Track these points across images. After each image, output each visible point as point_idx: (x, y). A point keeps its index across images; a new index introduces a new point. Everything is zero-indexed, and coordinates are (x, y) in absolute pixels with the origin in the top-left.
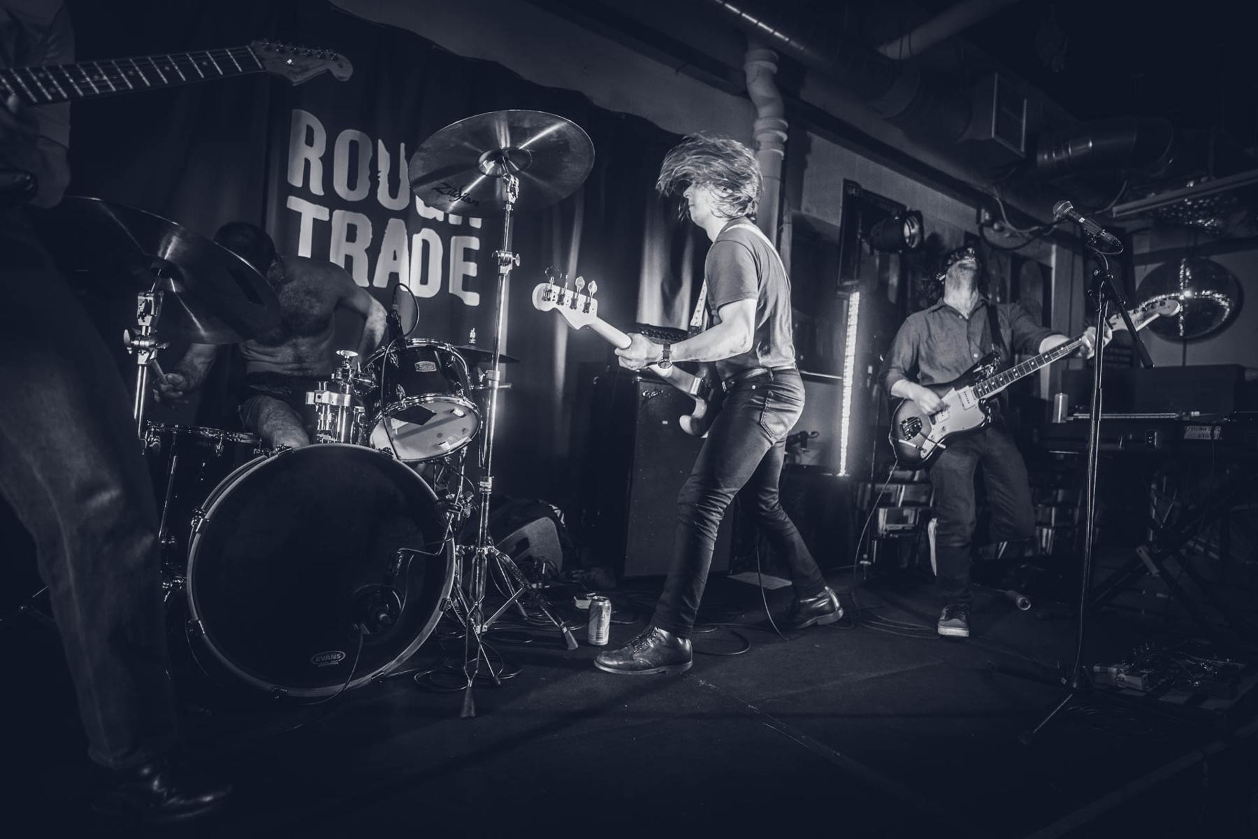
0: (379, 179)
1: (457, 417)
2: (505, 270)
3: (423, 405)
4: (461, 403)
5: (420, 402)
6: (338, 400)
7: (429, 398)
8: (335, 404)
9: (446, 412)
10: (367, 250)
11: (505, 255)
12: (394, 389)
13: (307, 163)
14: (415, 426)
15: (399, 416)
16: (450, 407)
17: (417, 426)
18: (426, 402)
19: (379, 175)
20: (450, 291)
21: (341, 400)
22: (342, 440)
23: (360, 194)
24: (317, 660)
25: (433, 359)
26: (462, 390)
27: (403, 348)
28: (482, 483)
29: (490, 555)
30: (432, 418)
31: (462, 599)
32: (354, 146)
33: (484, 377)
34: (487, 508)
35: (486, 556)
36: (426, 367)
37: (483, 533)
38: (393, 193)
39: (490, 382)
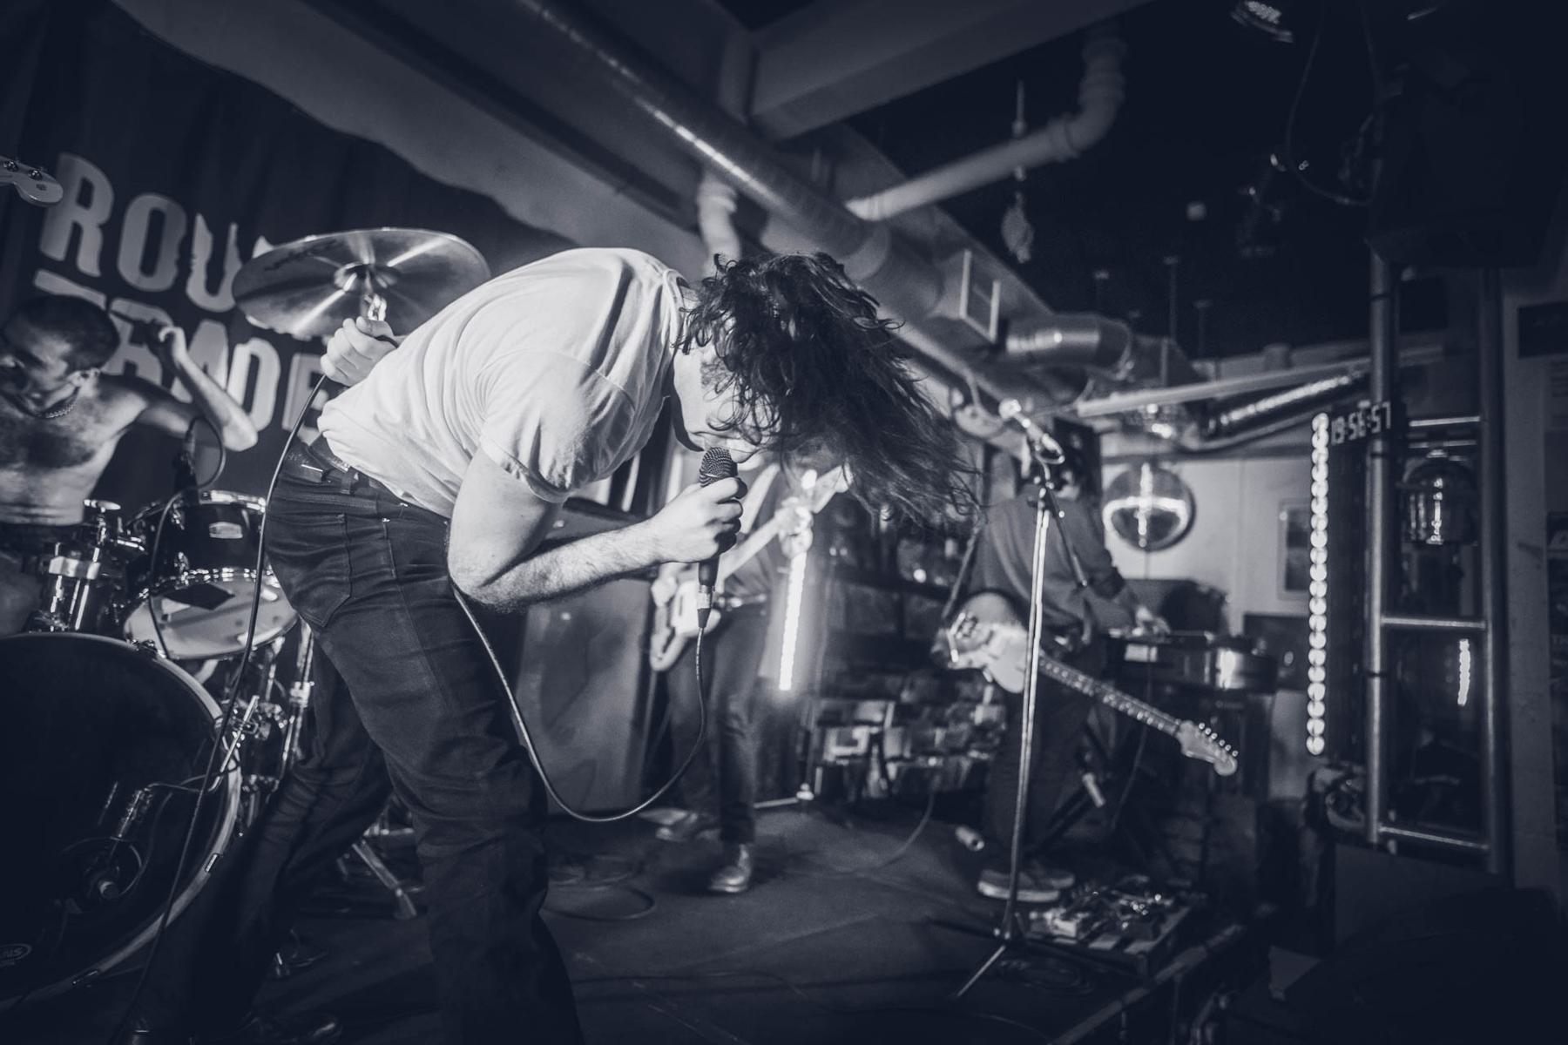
5: (212, 579)
6: (78, 570)
7: (227, 573)
8: (71, 574)
14: (199, 611)
15: (177, 597)
18: (220, 579)
23: (163, 279)
32: (157, 221)
36: (226, 530)
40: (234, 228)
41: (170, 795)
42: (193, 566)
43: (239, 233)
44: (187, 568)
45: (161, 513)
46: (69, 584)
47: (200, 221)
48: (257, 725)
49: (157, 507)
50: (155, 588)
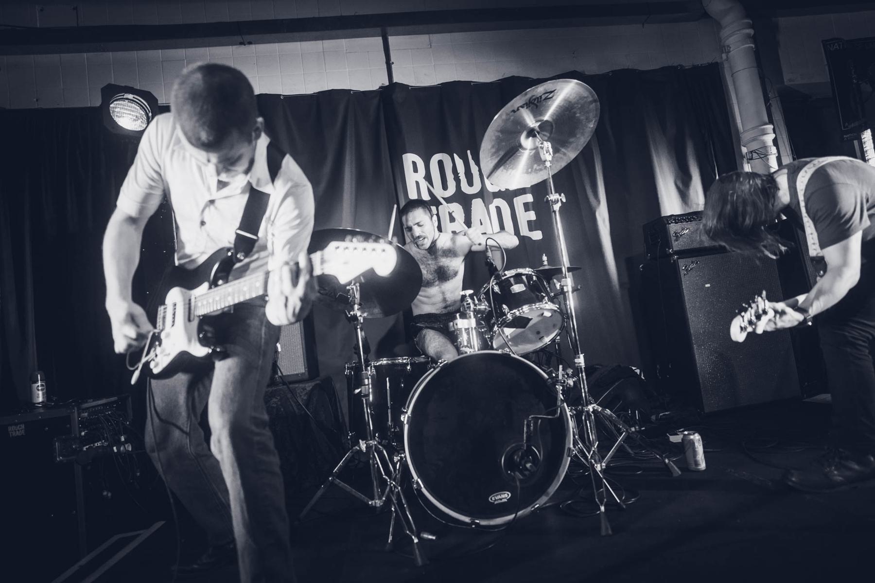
2: (557, 207)
5: (520, 313)
6: (468, 324)
7: (526, 308)
9: (539, 316)
11: (554, 196)
12: (501, 307)
13: (417, 183)
14: (520, 330)
15: (510, 325)
16: (541, 312)
18: (523, 312)
19: (459, 175)
20: (522, 235)
21: (470, 324)
22: (476, 349)
24: (493, 499)
25: (521, 282)
26: (546, 298)
27: (501, 280)
28: (576, 360)
29: (594, 411)
31: (582, 447)
33: (560, 285)
34: (585, 378)
35: (592, 412)
36: (518, 288)
37: (586, 396)
38: (470, 183)
39: (565, 287)
40: (469, 152)
41: (540, 421)
42: (511, 309)
44: (508, 311)
45: (489, 288)
47: (455, 156)
48: (566, 380)
49: (486, 287)
50: (499, 324)
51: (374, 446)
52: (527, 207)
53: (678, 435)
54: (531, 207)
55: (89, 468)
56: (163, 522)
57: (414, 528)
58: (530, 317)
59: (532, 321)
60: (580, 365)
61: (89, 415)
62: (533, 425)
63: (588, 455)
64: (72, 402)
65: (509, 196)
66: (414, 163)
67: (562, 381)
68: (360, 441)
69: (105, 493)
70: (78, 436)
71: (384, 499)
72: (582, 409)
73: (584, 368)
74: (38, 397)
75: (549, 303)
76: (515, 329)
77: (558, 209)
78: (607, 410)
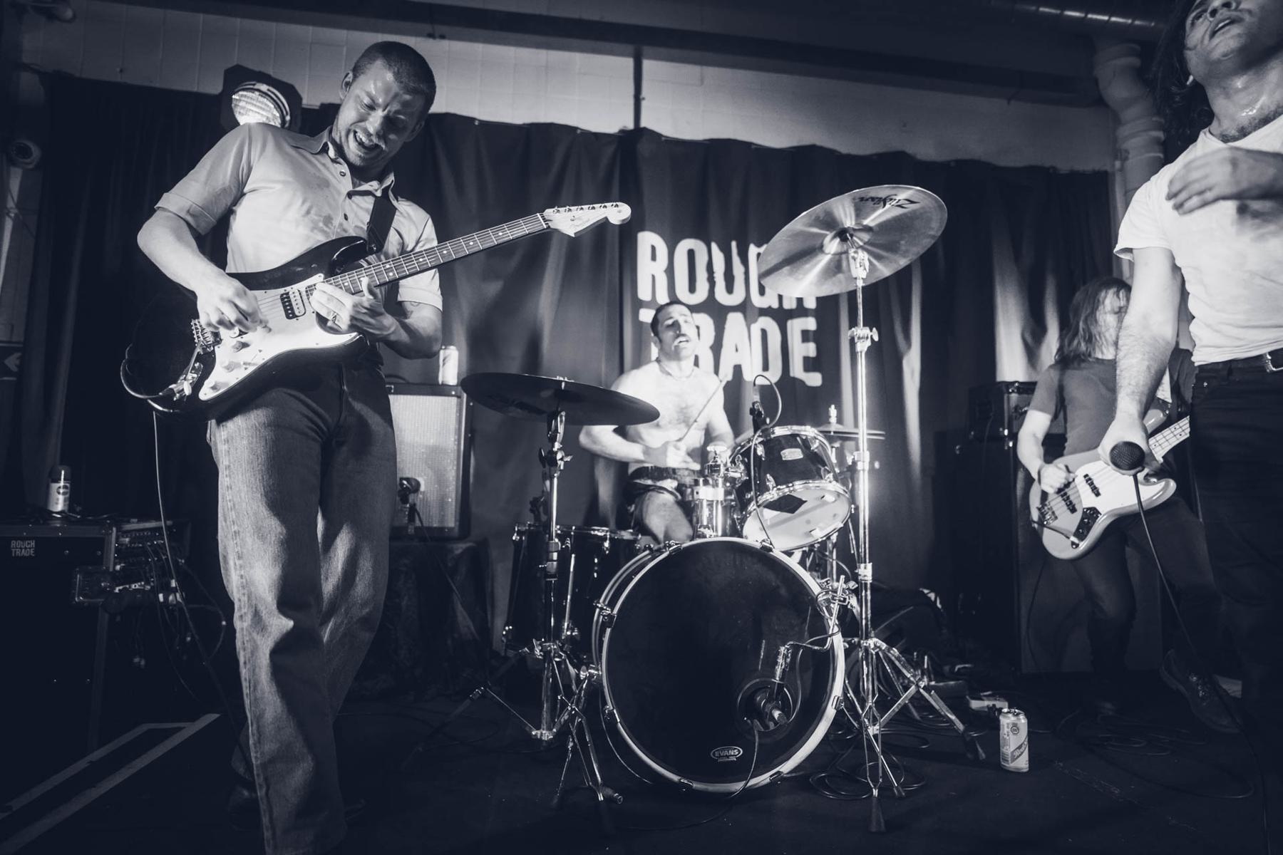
0: (715, 280)
1: (826, 503)
2: (862, 347)
3: (793, 494)
4: (829, 485)
9: (817, 499)
10: (712, 348)
17: (789, 515)
19: (715, 275)
22: (720, 533)
23: (701, 295)
24: (717, 754)
25: (797, 446)
27: (768, 438)
30: (803, 506)
31: (853, 696)
32: (691, 254)
34: (869, 598)
37: (866, 624)
40: (734, 244)
43: (738, 246)
44: (775, 485)
46: (710, 504)
47: (714, 246)
51: (553, 651)
52: (806, 336)
53: (983, 700)
54: (811, 336)
55: (118, 618)
56: (217, 716)
57: (599, 779)
58: (804, 499)
59: (805, 504)
60: (866, 578)
61: (130, 542)
62: (791, 656)
63: (861, 712)
64: (106, 519)
65: (782, 316)
66: (653, 248)
67: (842, 599)
68: (534, 640)
69: (136, 660)
70: (111, 570)
71: (555, 730)
72: (859, 642)
73: (871, 584)
74: (57, 504)
75: (834, 482)
76: (779, 512)
77: (866, 349)
78: (894, 649)
